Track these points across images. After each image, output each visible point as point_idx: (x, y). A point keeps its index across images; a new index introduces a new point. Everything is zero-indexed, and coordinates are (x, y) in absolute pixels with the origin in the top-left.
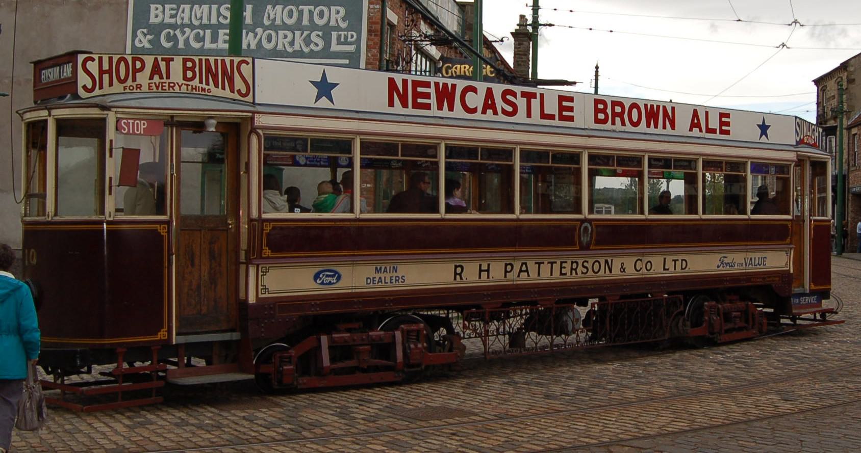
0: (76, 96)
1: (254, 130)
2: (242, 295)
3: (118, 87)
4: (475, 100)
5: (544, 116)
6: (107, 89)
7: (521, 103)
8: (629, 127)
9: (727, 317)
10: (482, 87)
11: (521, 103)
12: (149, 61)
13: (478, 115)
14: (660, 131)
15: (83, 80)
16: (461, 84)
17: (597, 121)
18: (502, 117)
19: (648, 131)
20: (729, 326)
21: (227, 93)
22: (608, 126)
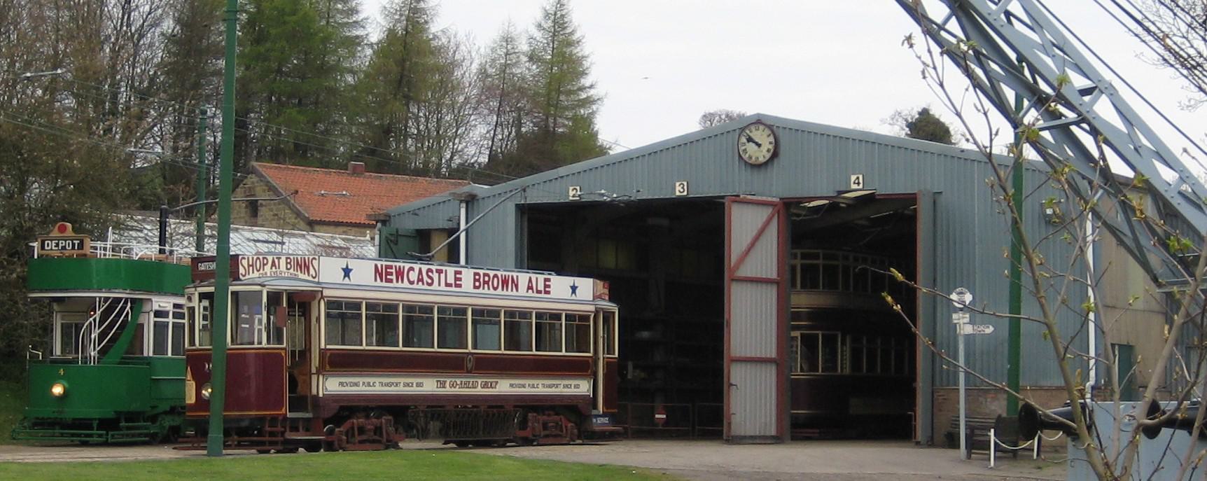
0: (238, 279)
1: (322, 297)
2: (314, 392)
3: (256, 274)
4: (414, 276)
5: (447, 285)
6: (251, 275)
7: (435, 276)
8: (492, 291)
9: (545, 426)
10: (417, 267)
11: (435, 276)
12: (270, 258)
13: (415, 286)
14: (509, 293)
15: (242, 270)
16: (407, 266)
17: (475, 287)
18: (426, 287)
19: (505, 292)
20: (547, 432)
21: (306, 277)
22: (480, 291)
